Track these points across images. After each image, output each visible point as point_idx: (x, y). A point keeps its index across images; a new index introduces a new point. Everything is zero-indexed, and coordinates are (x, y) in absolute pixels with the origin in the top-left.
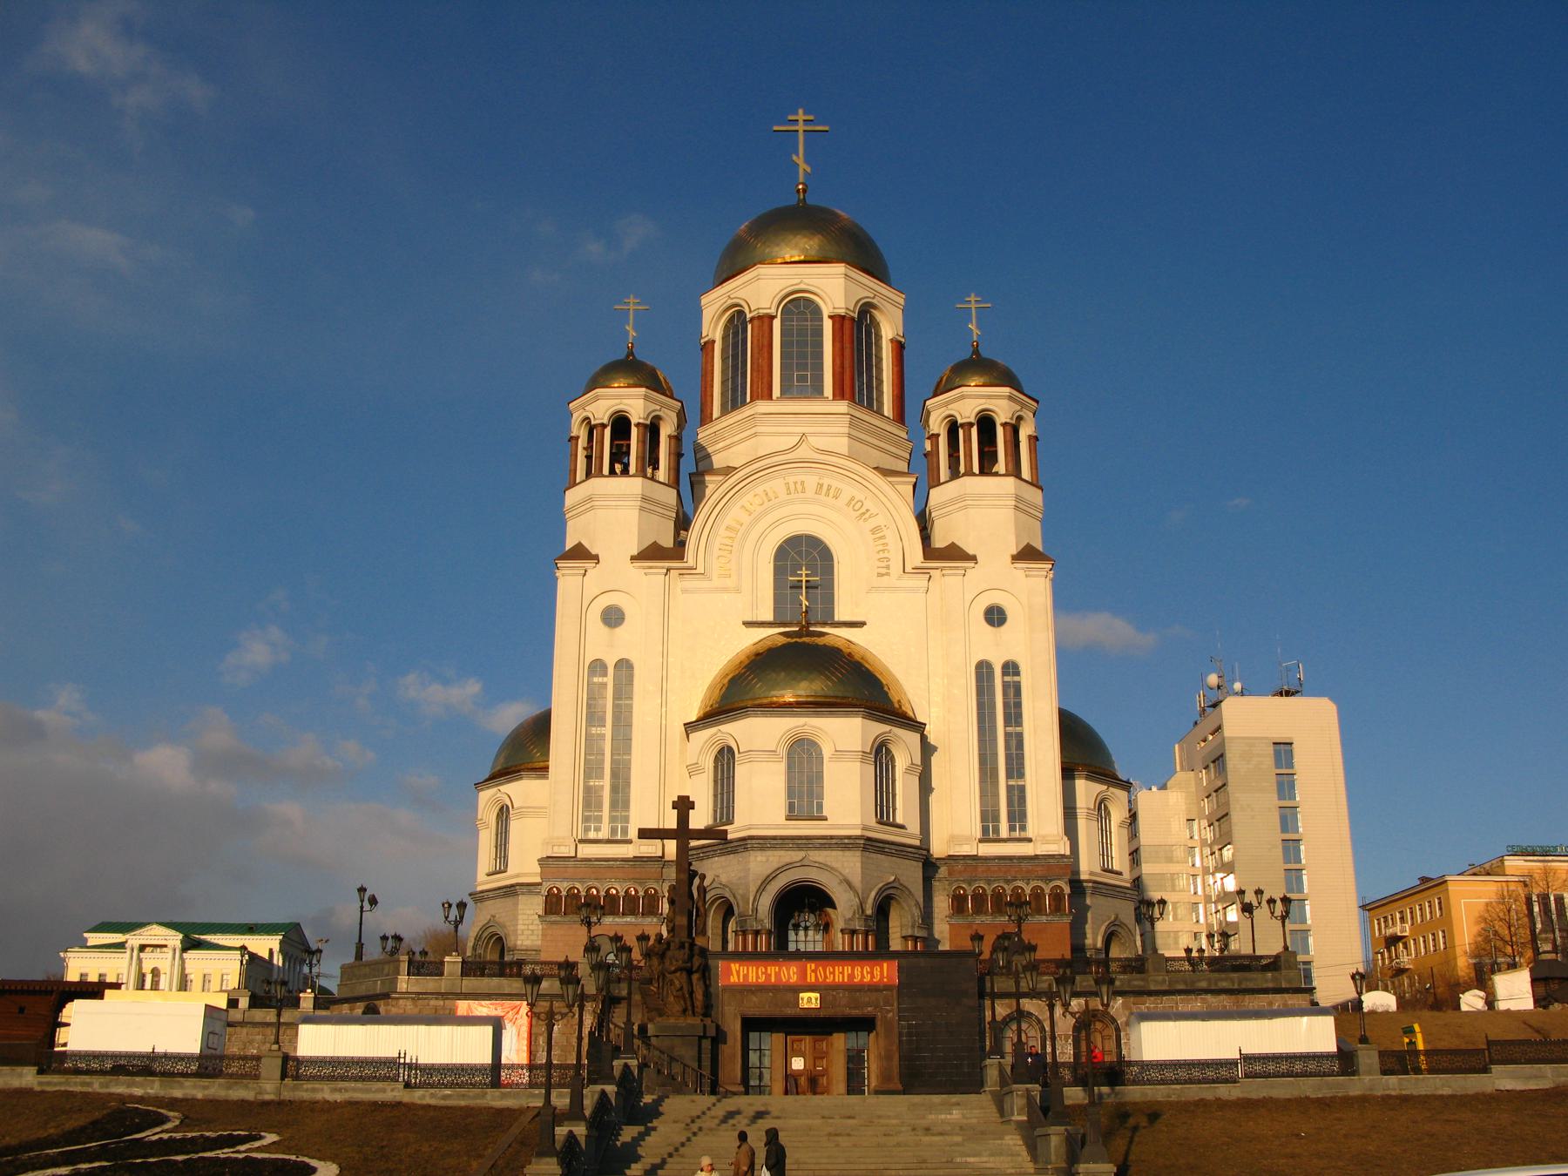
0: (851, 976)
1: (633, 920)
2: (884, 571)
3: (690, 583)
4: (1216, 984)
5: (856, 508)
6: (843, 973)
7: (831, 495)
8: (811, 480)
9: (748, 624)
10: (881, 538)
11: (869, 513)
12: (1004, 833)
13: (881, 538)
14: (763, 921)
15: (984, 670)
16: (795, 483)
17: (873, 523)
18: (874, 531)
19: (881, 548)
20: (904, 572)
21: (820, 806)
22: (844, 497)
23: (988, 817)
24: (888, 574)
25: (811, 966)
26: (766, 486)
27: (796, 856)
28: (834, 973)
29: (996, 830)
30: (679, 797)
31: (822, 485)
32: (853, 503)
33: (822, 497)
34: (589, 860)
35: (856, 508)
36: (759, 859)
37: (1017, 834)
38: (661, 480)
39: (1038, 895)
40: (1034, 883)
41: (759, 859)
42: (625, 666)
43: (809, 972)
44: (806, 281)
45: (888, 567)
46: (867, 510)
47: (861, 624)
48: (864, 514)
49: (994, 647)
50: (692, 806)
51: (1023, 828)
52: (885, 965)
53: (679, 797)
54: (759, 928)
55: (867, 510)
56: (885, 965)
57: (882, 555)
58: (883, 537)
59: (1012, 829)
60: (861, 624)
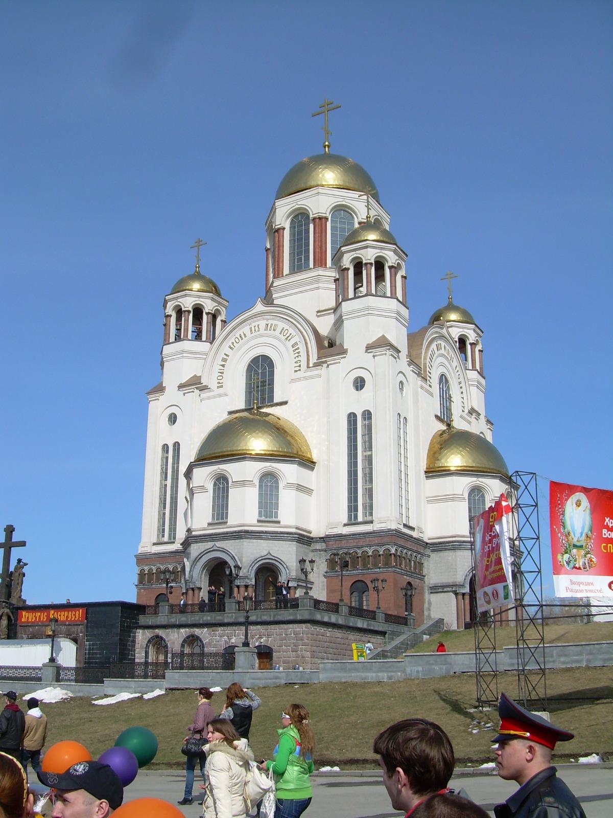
0: (67, 617)
1: (175, 585)
2: (298, 368)
3: (205, 394)
4: (261, 618)
5: (284, 334)
6: (64, 615)
7: (272, 330)
8: (262, 324)
9: (230, 413)
10: (296, 349)
11: (291, 336)
12: (360, 519)
13: (296, 349)
14: (195, 582)
15: (352, 418)
16: (255, 327)
17: (293, 341)
18: (293, 346)
19: (297, 355)
20: (308, 367)
21: (227, 518)
22: (279, 329)
23: (353, 508)
24: (300, 370)
25: (52, 612)
26: (241, 332)
27: (209, 545)
28: (60, 616)
29: (356, 517)
30: (7, 526)
31: (267, 325)
32: (283, 331)
33: (268, 332)
34: (155, 554)
35: (284, 334)
36: (195, 547)
37: (369, 518)
38: (190, 338)
39: (376, 555)
40: (373, 548)
41: (195, 547)
42: (177, 446)
43: (51, 615)
44: (299, 203)
45: (300, 366)
46: (290, 334)
47: (285, 403)
48: (288, 337)
49: (358, 403)
50: (13, 530)
51: (371, 514)
52: (81, 610)
53: (7, 526)
54: (194, 586)
55: (290, 334)
56: (81, 610)
57: (297, 359)
58: (298, 348)
59: (365, 515)
60: (285, 403)
